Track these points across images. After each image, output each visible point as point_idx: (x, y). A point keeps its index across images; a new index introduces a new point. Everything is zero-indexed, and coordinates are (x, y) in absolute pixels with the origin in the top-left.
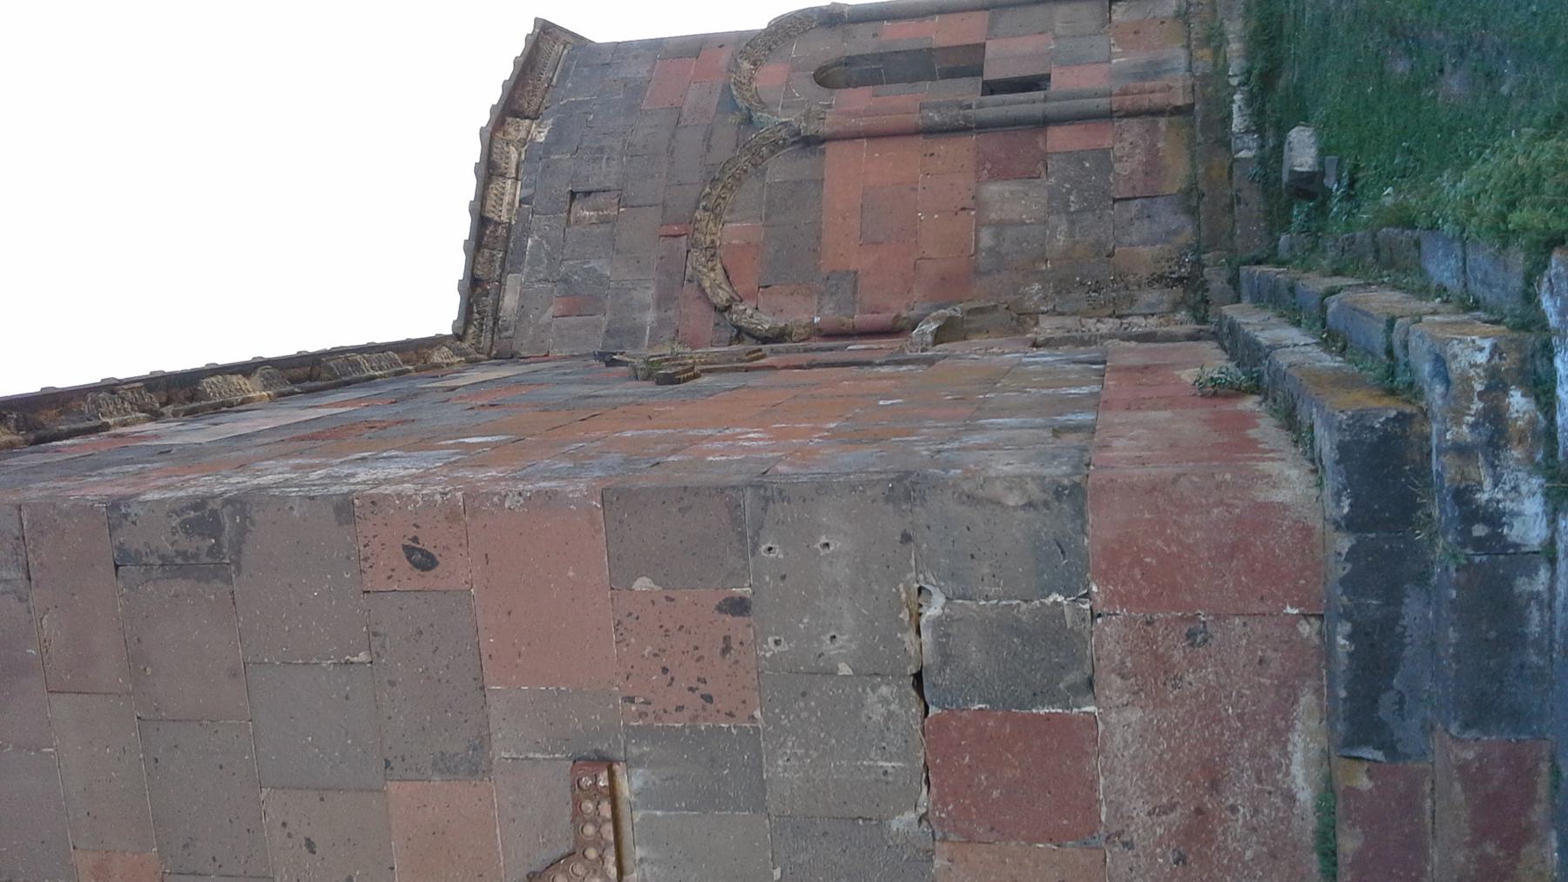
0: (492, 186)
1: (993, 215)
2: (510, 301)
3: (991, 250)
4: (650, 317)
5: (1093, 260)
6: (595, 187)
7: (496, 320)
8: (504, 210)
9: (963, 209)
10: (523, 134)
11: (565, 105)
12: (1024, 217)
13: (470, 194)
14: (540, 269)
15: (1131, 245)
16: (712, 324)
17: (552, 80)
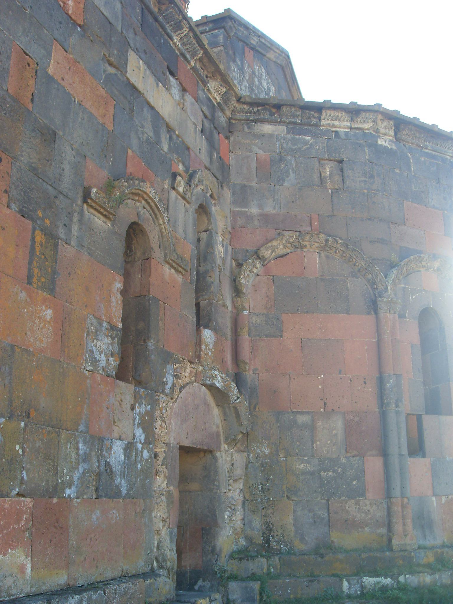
0: (344, 114)
1: (319, 424)
2: (267, 128)
3: (295, 422)
4: (254, 210)
5: (284, 487)
6: (345, 174)
7: (256, 121)
8: (329, 122)
9: (325, 404)
10: (382, 131)
11: (407, 156)
12: (318, 443)
13: (337, 99)
14: (290, 144)
15: (295, 511)
16: (248, 248)
17: (426, 149)
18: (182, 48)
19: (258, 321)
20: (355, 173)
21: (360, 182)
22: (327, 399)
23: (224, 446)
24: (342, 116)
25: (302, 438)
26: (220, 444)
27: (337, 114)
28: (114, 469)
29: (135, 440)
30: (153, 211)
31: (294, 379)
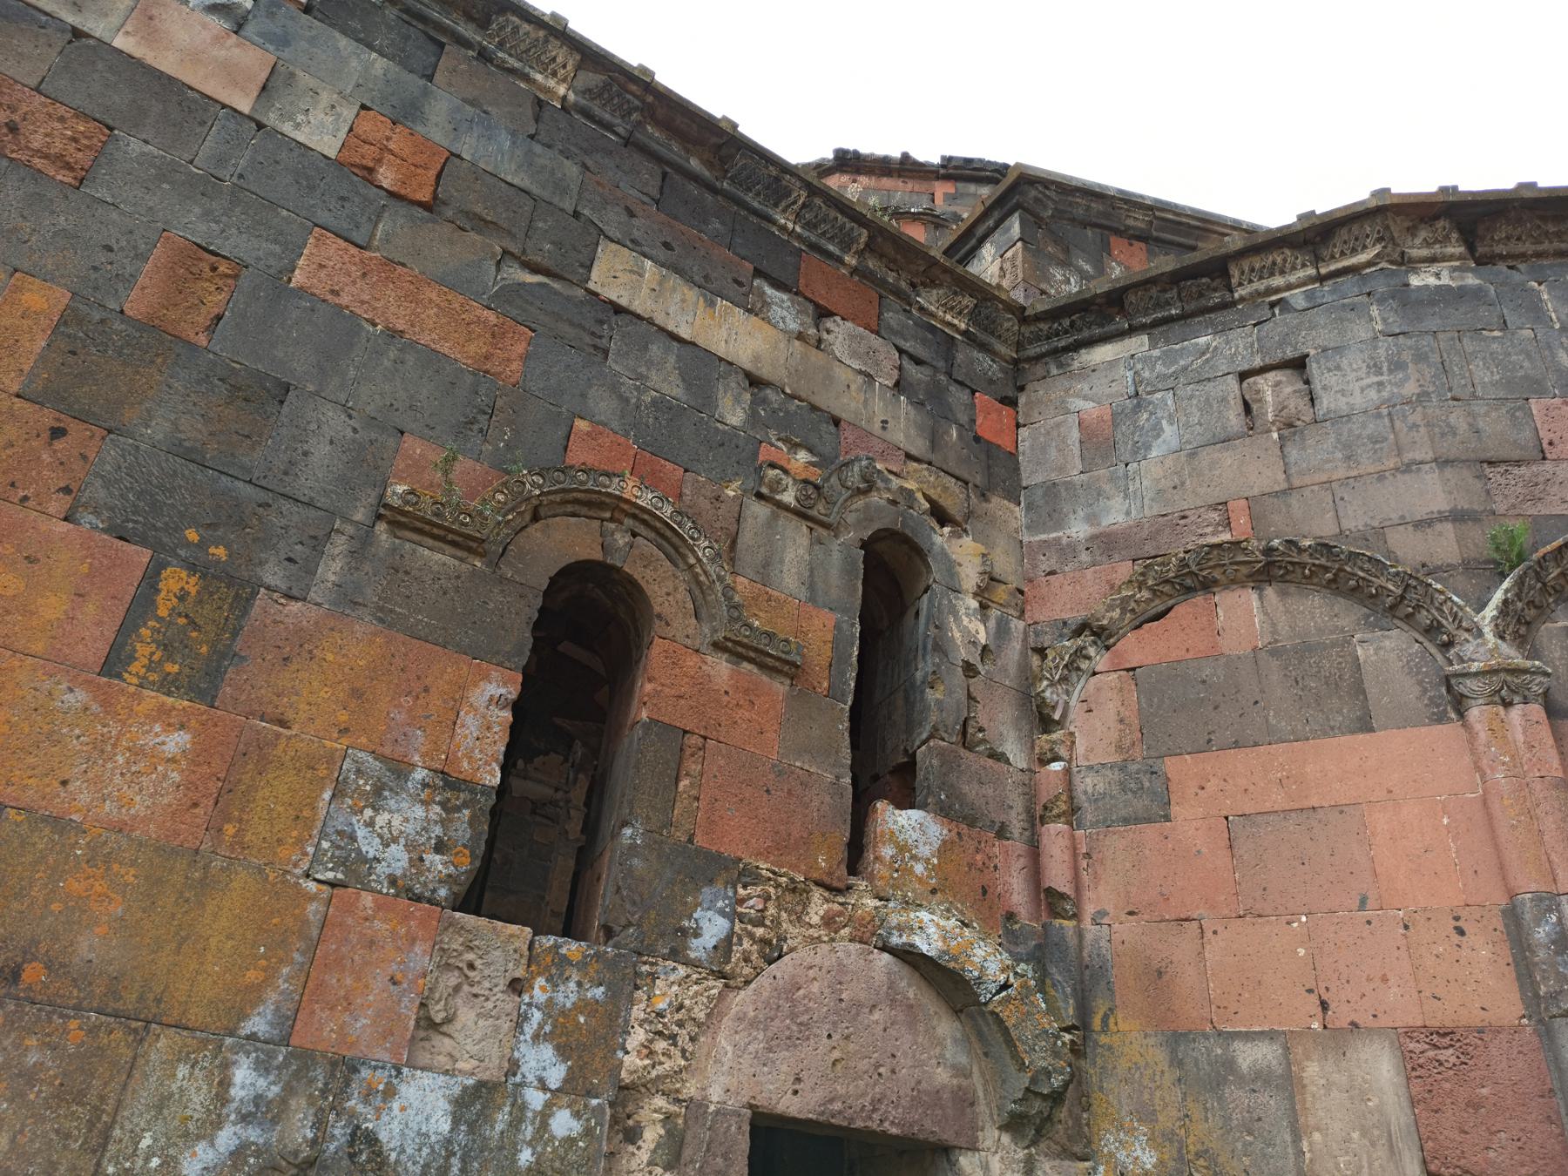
0: (1288, 252)
1: (1312, 1070)
3: (1230, 1064)
7: (1077, 347)
9: (1324, 1006)
12: (1317, 1136)
14: (1159, 368)
16: (1065, 616)
18: (806, 234)
19: (1101, 787)
20: (1344, 376)
21: (1362, 390)
22: (1327, 989)
23: (990, 1135)
24: (1285, 260)
25: (1260, 1119)
26: (975, 1128)
27: (1271, 258)
28: (393, 1156)
29: (518, 1079)
30: (662, 536)
31: (1215, 932)
